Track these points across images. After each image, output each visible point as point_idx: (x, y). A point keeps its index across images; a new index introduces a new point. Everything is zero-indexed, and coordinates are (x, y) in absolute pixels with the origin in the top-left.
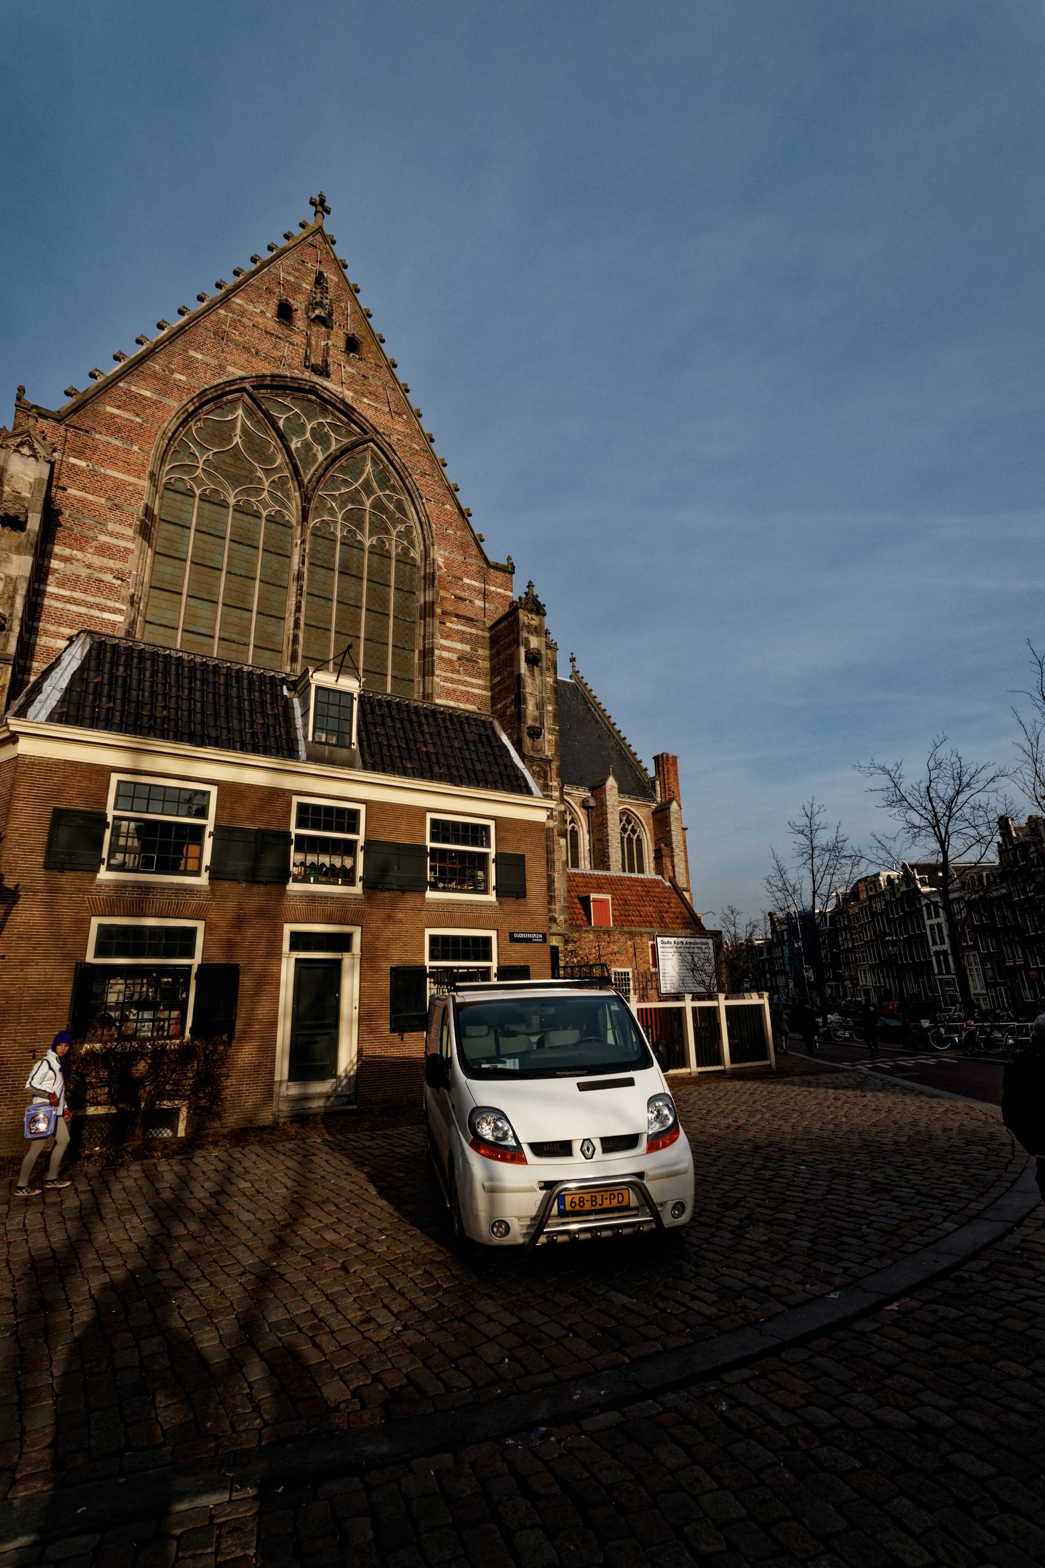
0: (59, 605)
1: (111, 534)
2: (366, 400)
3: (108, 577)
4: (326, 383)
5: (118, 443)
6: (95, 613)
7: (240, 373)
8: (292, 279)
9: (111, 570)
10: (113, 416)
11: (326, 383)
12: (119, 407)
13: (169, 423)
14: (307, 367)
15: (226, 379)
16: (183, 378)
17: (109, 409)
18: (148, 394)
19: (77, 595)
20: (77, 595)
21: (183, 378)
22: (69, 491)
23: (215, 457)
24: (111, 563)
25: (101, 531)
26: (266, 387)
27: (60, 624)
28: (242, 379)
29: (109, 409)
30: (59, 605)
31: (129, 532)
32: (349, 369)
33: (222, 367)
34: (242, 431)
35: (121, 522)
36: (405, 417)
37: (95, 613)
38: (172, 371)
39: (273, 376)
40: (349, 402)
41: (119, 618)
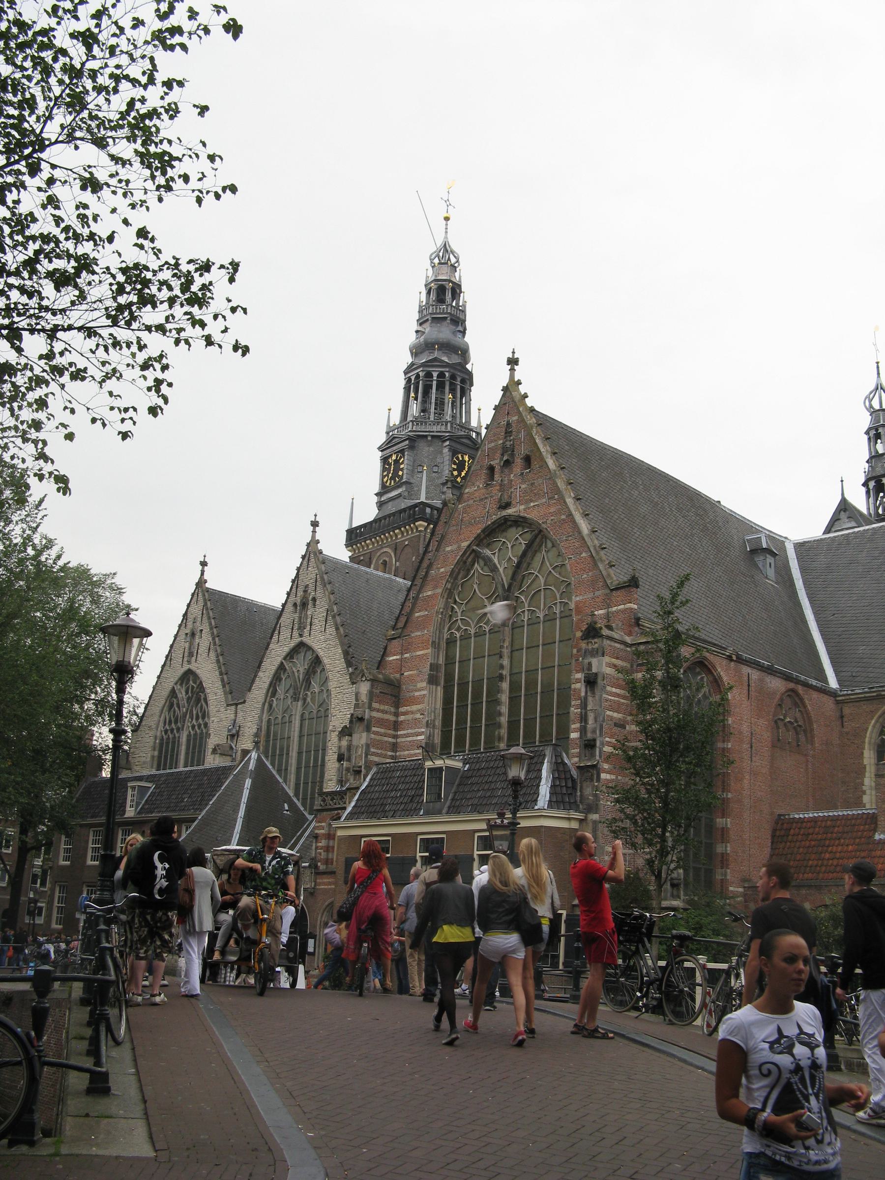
0: (403, 740)
1: (420, 690)
2: (532, 504)
3: (418, 716)
4: (510, 511)
5: (419, 633)
6: (415, 738)
7: (465, 544)
8: (493, 444)
9: (419, 710)
10: (418, 617)
11: (510, 511)
12: (420, 611)
13: (440, 604)
14: (499, 508)
15: (461, 553)
16: (442, 570)
17: (417, 615)
18: (429, 593)
19: (410, 731)
20: (410, 731)
21: (442, 570)
22: (406, 674)
23: (468, 605)
24: (419, 707)
25: (416, 691)
26: (485, 538)
27: (404, 750)
28: (469, 546)
29: (417, 615)
30: (403, 740)
31: (424, 684)
32: (523, 486)
33: (459, 547)
34: (478, 578)
35: (422, 681)
36: (556, 496)
37: (415, 738)
38: (439, 569)
39: (483, 531)
40: (522, 514)
41: (422, 737)
